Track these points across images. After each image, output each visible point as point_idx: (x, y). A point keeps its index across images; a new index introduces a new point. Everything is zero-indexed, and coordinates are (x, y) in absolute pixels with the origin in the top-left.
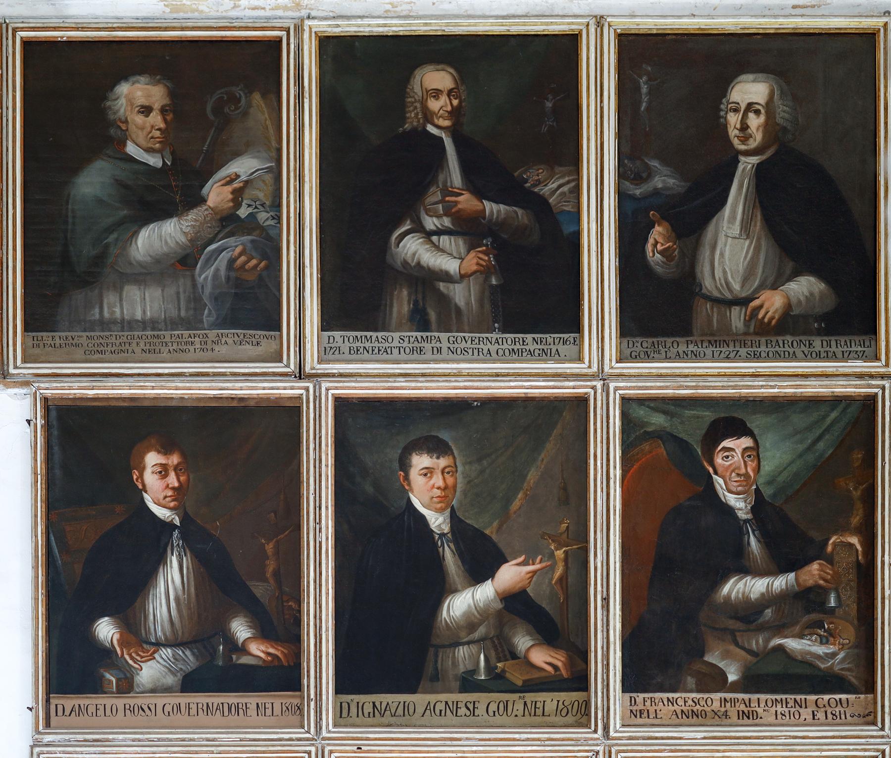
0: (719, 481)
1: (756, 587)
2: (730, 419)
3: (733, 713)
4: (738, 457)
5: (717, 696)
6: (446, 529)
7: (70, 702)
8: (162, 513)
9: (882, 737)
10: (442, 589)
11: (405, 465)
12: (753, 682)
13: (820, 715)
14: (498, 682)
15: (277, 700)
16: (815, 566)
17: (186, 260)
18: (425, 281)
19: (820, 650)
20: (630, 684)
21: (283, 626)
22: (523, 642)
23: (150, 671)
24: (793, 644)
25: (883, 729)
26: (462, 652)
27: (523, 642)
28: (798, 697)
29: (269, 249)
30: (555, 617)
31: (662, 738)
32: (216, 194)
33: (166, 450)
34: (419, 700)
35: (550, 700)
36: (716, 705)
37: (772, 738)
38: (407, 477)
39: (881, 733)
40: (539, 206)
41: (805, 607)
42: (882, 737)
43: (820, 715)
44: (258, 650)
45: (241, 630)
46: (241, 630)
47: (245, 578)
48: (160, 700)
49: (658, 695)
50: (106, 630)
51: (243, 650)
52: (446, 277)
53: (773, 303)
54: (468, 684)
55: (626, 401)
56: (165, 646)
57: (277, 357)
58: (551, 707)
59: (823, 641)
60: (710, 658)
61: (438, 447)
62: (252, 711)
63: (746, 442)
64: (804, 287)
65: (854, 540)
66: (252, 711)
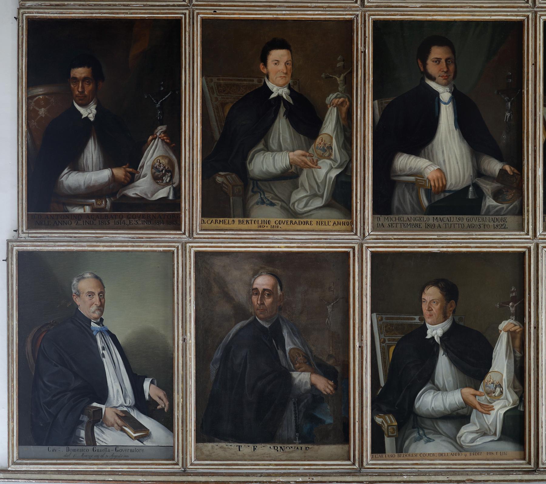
9: (527, 7)
31: (396, 7)
37: (461, 7)
39: (527, 5)
42: (527, 7)
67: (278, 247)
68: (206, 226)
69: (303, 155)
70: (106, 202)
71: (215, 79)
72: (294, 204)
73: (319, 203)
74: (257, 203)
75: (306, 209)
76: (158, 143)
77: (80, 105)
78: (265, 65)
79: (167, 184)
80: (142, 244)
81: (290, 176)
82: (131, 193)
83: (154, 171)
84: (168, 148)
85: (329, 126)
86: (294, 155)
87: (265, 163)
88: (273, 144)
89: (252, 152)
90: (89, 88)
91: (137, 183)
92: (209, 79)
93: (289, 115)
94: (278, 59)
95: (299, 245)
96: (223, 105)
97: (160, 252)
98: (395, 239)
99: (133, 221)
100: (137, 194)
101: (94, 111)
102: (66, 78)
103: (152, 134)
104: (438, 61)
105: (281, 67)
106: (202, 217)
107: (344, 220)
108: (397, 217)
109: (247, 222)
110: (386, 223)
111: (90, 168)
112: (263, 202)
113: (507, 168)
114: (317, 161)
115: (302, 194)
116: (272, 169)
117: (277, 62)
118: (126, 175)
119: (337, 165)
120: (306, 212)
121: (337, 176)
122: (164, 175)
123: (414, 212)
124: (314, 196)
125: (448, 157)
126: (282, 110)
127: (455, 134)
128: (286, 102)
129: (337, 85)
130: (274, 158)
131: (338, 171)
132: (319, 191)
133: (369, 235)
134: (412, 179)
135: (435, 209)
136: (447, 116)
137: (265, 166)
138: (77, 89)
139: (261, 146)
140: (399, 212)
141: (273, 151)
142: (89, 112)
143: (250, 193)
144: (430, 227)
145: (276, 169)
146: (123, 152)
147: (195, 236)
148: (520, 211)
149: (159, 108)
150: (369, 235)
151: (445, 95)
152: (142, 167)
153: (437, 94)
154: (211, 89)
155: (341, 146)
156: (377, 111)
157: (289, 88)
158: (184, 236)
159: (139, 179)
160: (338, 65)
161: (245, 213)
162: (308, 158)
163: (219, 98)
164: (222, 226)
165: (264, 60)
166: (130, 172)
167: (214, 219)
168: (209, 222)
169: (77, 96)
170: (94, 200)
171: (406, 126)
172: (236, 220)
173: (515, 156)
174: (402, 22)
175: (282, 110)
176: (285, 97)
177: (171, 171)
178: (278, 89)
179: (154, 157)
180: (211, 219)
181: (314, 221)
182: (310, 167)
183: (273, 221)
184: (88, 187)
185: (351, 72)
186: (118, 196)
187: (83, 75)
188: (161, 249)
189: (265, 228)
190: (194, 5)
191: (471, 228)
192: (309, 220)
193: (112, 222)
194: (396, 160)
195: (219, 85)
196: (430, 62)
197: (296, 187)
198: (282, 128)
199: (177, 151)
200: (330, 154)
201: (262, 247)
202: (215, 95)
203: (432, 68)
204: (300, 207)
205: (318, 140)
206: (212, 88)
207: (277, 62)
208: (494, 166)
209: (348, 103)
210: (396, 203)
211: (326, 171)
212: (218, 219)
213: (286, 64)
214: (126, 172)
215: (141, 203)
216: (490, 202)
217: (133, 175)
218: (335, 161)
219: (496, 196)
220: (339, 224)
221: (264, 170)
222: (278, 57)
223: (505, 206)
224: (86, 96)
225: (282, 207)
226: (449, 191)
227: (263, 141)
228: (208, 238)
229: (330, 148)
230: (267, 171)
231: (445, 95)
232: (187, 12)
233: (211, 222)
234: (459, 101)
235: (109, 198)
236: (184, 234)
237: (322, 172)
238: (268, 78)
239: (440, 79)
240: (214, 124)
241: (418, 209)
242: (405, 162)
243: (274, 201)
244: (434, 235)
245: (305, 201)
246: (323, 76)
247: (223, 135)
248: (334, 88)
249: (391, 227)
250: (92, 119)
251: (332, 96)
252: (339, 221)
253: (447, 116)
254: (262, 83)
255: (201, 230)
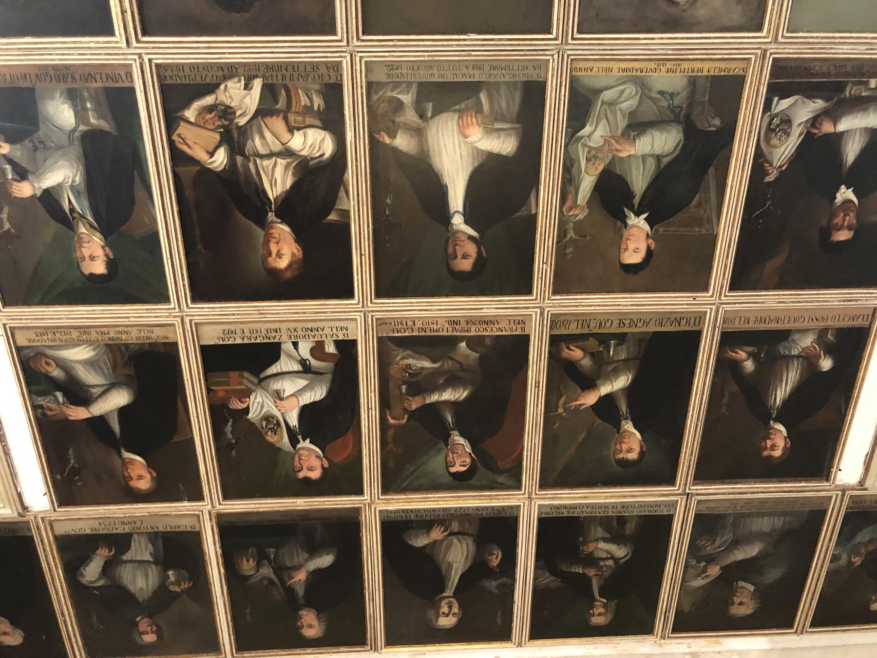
0: (468, 449)
1: (448, 395)
2: (460, 482)
3: (463, 324)
4: (458, 462)
5: (473, 333)
6: (623, 422)
7: (859, 323)
8: (780, 427)
10: (628, 391)
11: (642, 453)
12: (451, 342)
13: (410, 323)
14: (604, 339)
15: (737, 326)
16: (414, 407)
17: (736, 543)
18: (616, 538)
19: (410, 361)
20: (526, 339)
21: (725, 367)
22: (586, 362)
23: (807, 341)
24: (427, 364)
25: (372, 316)
26: (623, 356)
27: (586, 362)
28: (424, 334)
29: (694, 549)
30: (565, 375)
31: (507, 308)
32: (714, 571)
33: (770, 457)
34: (653, 328)
35: (573, 329)
36: (473, 329)
37: (441, 310)
38: (642, 447)
40: (555, 572)
41: (419, 384)
42: (372, 311)
43: (410, 323)
44: (742, 355)
45: (749, 366)
46: (749, 366)
47: (740, 393)
48: (805, 325)
49: (508, 333)
50: (826, 364)
51: (750, 355)
52: (605, 540)
53: (436, 534)
54: (621, 338)
55: (518, 487)
56: (795, 356)
57: (699, 502)
58: (573, 326)
59: (409, 366)
60: (477, 355)
61: (624, 463)
62: (752, 319)
63: (453, 470)
64: (420, 541)
65: (392, 421)
66: (752, 319)
67: (662, 38)
68: (742, 65)
69: (620, 151)
70: (850, 93)
71: (704, 231)
72: (636, 94)
73: (607, 95)
74: (678, 93)
75: (622, 88)
76: (777, 163)
77: (852, 201)
78: (648, 247)
79: (776, 115)
80: (824, 40)
81: (637, 126)
82: (819, 104)
83: (789, 130)
84: (768, 157)
85: (587, 183)
86: (629, 151)
87: (663, 142)
88: (651, 164)
89: (676, 154)
90: (838, 220)
91: (811, 115)
92: (710, 232)
93: (631, 195)
94: (634, 253)
95: (638, 42)
96: (699, 205)
97: (802, 31)
98: (522, 50)
99: (825, 69)
100: (814, 102)
101: (838, 195)
102: (859, 230)
103: (781, 172)
104: (465, 256)
105: (632, 246)
106: (745, 76)
107: (580, 74)
108: (517, 79)
109: (693, 71)
110: (530, 70)
111: (858, 132)
112: (672, 95)
113: (387, 140)
114: (604, 145)
115: (625, 106)
116: (656, 134)
117: (636, 250)
118: (821, 124)
119: (583, 141)
120: (624, 83)
121: (583, 127)
122: (778, 126)
123: (497, 84)
124: (611, 104)
125: (456, 151)
126: (636, 201)
127: (447, 180)
128: (631, 208)
129: (574, 228)
130: (653, 146)
131: (582, 133)
132: (606, 111)
133: (553, 55)
134: (498, 126)
135: (471, 89)
136: (457, 199)
137: (664, 138)
138: (851, 218)
139: (665, 161)
140: (515, 84)
141: (652, 155)
142: (845, 194)
143: (684, 106)
144: (478, 65)
145: (652, 134)
146: (819, 150)
147: (759, 52)
148: (371, 86)
149: (768, 200)
150: (553, 55)
151: (458, 221)
152: (800, 135)
153: (467, 222)
154: (710, 221)
155: (576, 165)
156: (533, 201)
157: (626, 225)
158: (772, 51)
159: (806, 121)
160: (571, 249)
161: (693, 82)
162: (613, 148)
163: (702, 212)
164: (723, 65)
165: (649, 253)
166: (816, 128)
167: (731, 73)
168: (737, 70)
169: (853, 211)
170: (863, 94)
171: (503, 188)
172: (705, 73)
173: (378, 153)
174: (502, 294)
175: (636, 201)
176: (632, 215)
177: (770, 130)
178: (639, 223)
179: (785, 146)
180: (734, 73)
181: (615, 70)
182: (613, 137)
183: (663, 73)
184: (866, 110)
185: (558, 242)
186: (836, 99)
187: (841, 232)
188: (801, 34)
189: (673, 63)
190: (714, 304)
191: (428, 65)
192: (621, 74)
193: (849, 68)
194: (515, 148)
195: (701, 225)
196: (474, 255)
197: (632, 114)
198: (639, 181)
199: (759, 154)
200: (589, 152)
201: (682, 38)
202: (706, 215)
203: (471, 249)
204: (630, 89)
205: (600, 168)
206: (708, 222)
207: (636, 250)
208: (402, 142)
209: (564, 209)
210: (518, 96)
211: (595, 133)
212: (726, 73)
213: (626, 249)
214: (819, 129)
215: (810, 91)
216: (407, 99)
217: (813, 126)
218: (584, 145)
219: (399, 106)
220: (586, 70)
221: (664, 134)
222: (633, 255)
223: (389, 94)
224: (844, 211)
225: (650, 90)
226: (455, 111)
227: (662, 166)
228: (744, 49)
229: (588, 160)
230: (662, 133)
231: (458, 221)
232: (723, 298)
233: (736, 69)
234: (443, 215)
235: (846, 98)
236: (771, 54)
237: (599, 132)
238: (648, 235)
239: (463, 238)
240: (713, 185)
241: (491, 87)
242: (504, 145)
243: (659, 96)
244: (476, 56)
245: (622, 99)
246: (588, 238)
247: (705, 171)
248: (579, 226)
249: (524, 65)
250: (843, 186)
251: (581, 217)
252: (586, 73)
253: (457, 199)
254: (654, 228)
255: (749, 59)
